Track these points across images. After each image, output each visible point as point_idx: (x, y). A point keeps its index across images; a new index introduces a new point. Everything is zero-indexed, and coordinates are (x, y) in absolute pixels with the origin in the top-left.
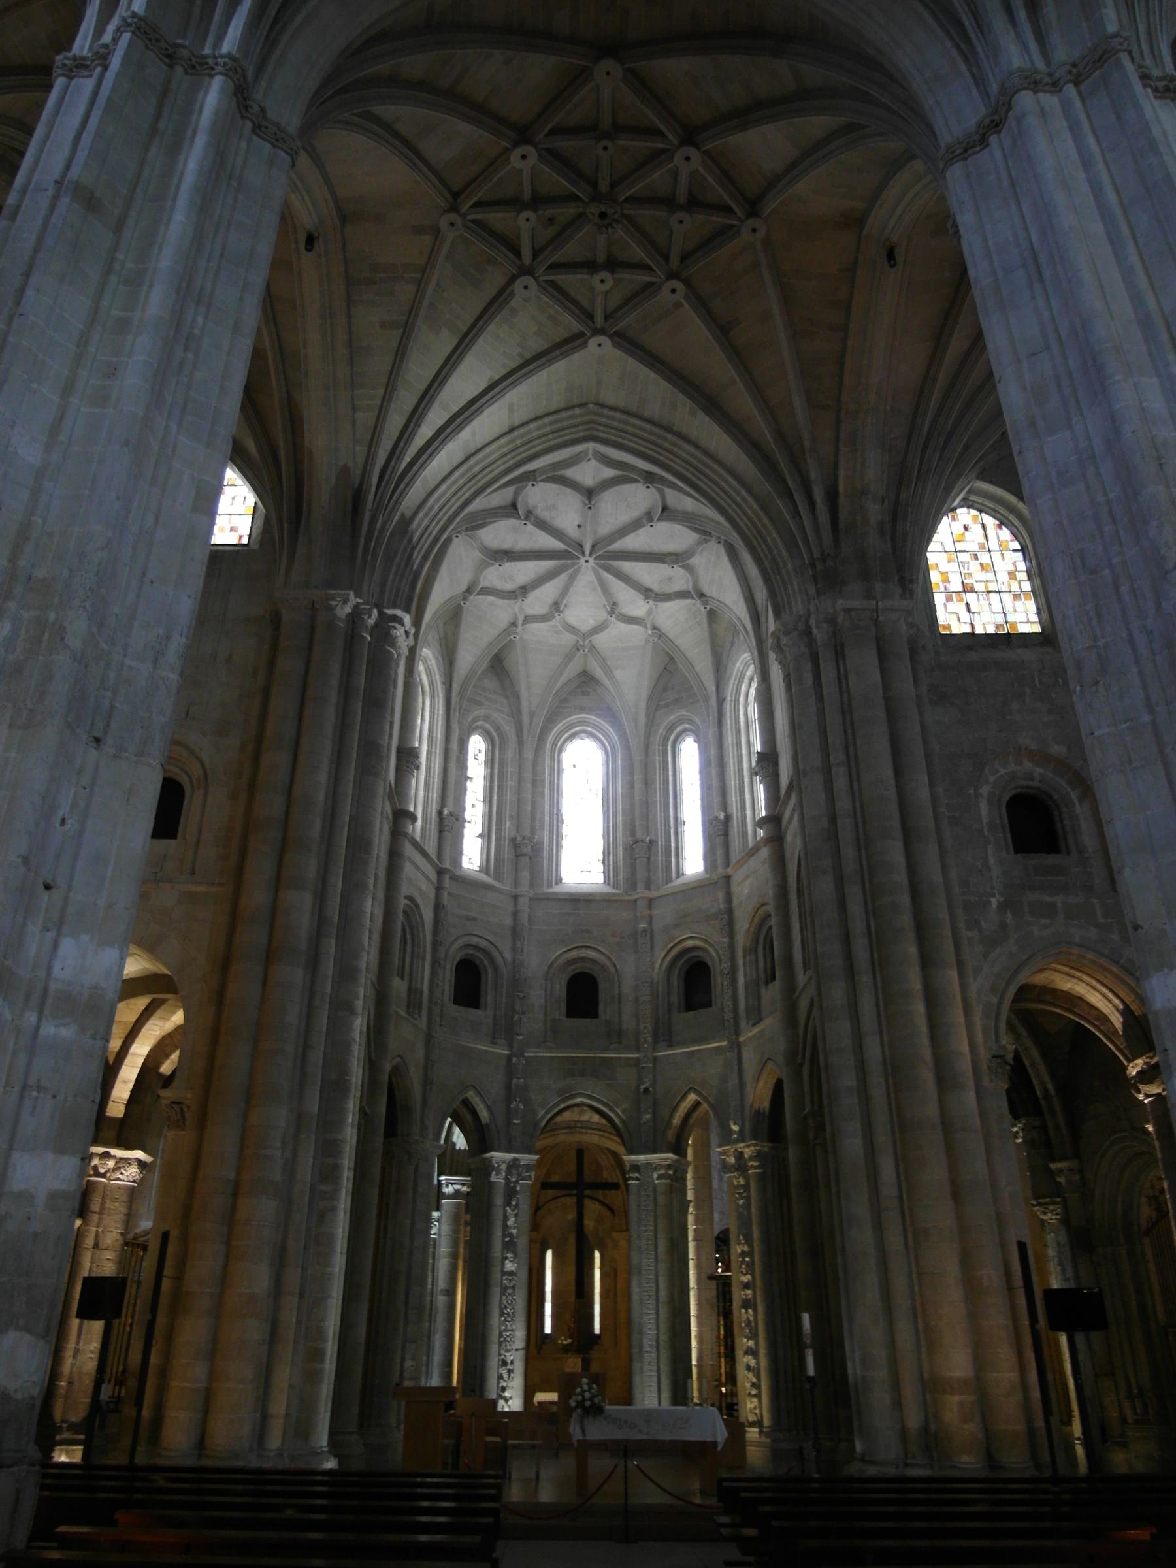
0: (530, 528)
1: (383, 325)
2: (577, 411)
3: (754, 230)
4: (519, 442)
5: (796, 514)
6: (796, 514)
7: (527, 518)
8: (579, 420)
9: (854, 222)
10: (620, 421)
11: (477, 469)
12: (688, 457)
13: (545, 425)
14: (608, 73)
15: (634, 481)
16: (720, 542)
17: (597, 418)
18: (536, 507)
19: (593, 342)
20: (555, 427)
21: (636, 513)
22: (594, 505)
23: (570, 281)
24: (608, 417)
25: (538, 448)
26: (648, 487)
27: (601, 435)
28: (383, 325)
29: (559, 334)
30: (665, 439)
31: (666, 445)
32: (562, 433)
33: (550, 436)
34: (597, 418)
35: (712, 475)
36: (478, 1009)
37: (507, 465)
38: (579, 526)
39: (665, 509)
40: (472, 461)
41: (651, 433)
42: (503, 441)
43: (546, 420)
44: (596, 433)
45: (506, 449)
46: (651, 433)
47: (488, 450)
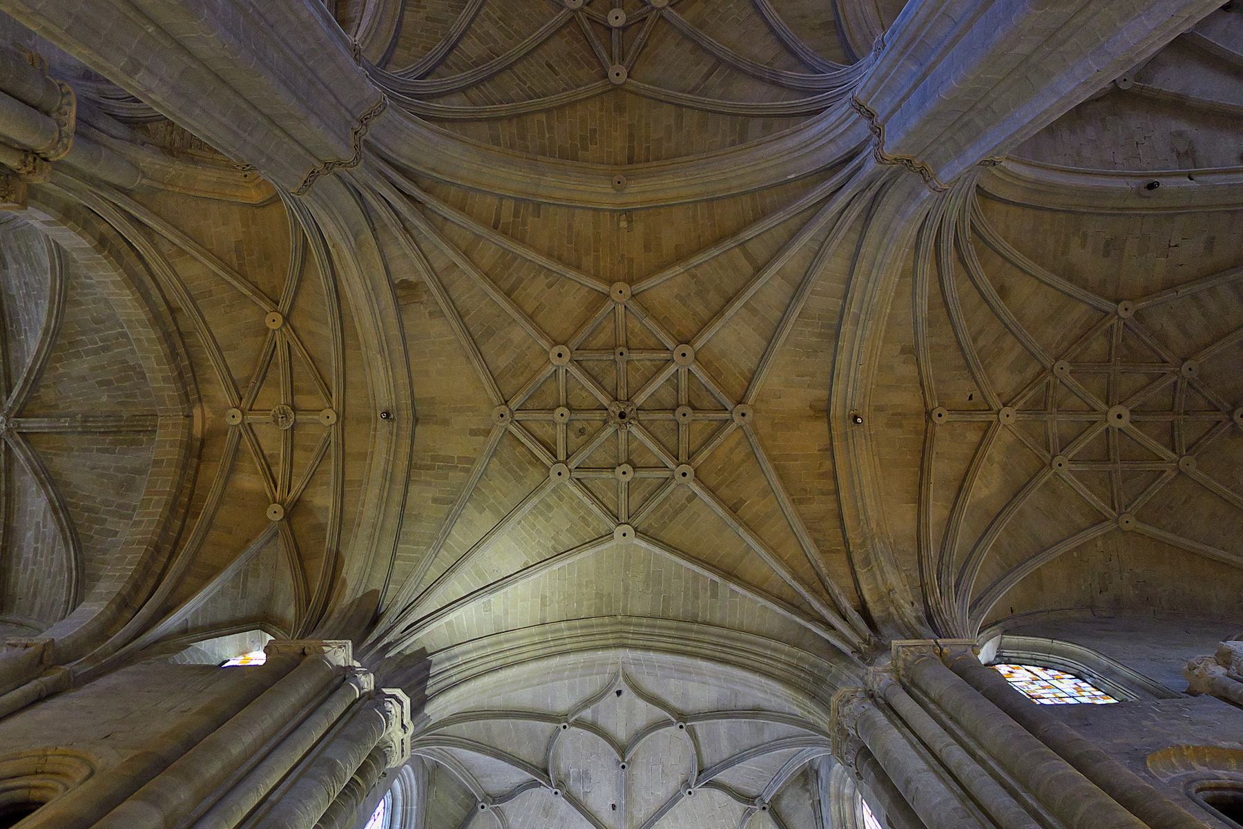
0: (563, 805)
1: (435, 500)
2: (607, 620)
3: (743, 415)
4: (550, 637)
5: (830, 627)
6: (830, 627)
7: (558, 786)
8: (608, 629)
9: (822, 411)
10: (647, 626)
11: (506, 646)
12: (715, 639)
13: (576, 628)
14: (621, 292)
15: (667, 723)
16: (764, 808)
17: (626, 628)
18: (568, 775)
19: (618, 531)
20: (585, 631)
21: (673, 784)
22: (628, 763)
23: (597, 480)
24: (635, 625)
25: (569, 647)
26: (681, 727)
27: (630, 642)
28: (435, 500)
29: (590, 533)
30: (691, 631)
31: (693, 636)
32: (593, 638)
33: (581, 639)
34: (626, 628)
35: (739, 645)
36: (424, 648)
37: (537, 653)
38: (614, 807)
39: (700, 773)
40: (502, 636)
41: (677, 629)
42: (533, 630)
43: (577, 623)
44: (625, 641)
45: (536, 639)
46: (677, 629)
47: (518, 633)
